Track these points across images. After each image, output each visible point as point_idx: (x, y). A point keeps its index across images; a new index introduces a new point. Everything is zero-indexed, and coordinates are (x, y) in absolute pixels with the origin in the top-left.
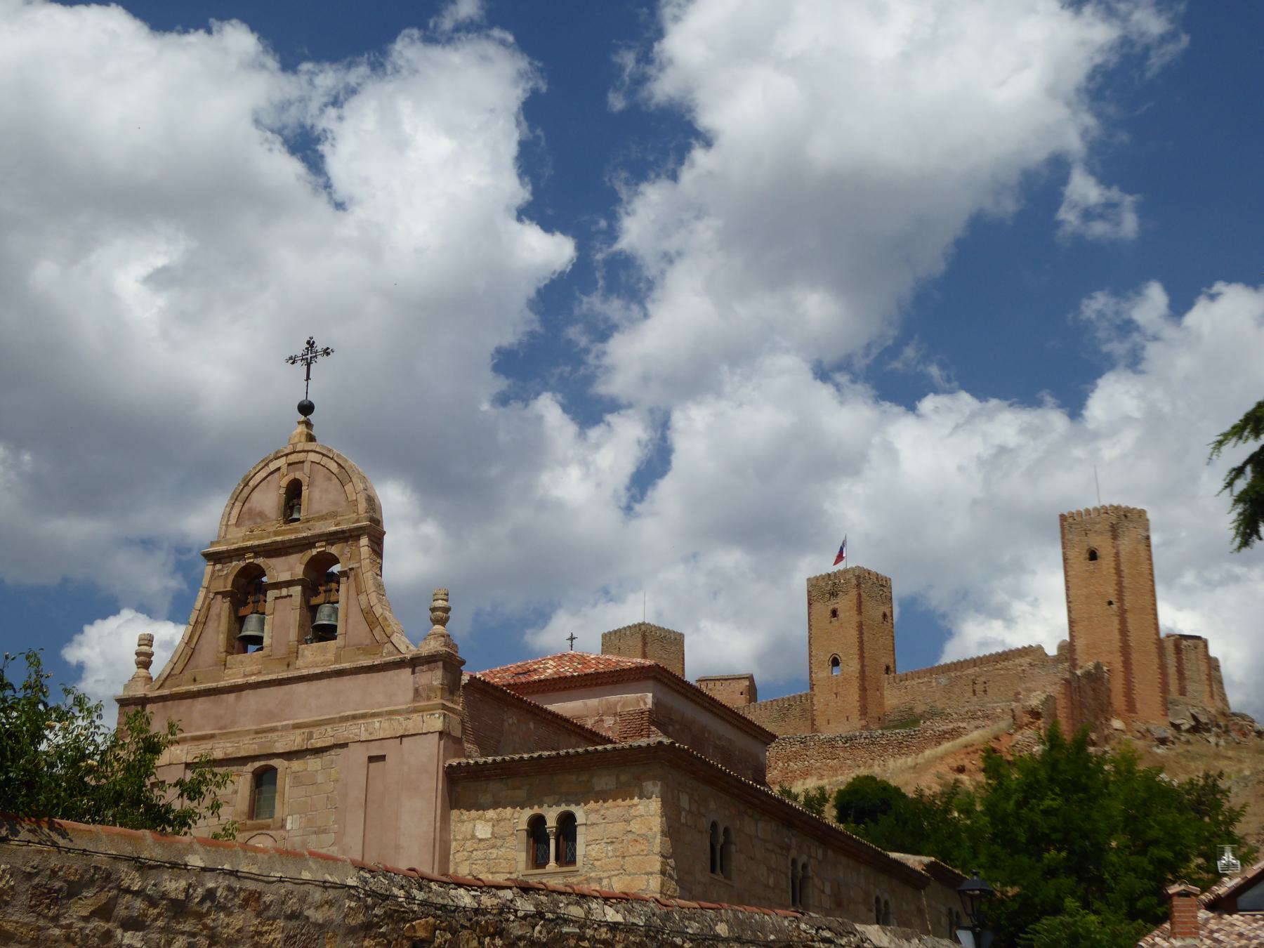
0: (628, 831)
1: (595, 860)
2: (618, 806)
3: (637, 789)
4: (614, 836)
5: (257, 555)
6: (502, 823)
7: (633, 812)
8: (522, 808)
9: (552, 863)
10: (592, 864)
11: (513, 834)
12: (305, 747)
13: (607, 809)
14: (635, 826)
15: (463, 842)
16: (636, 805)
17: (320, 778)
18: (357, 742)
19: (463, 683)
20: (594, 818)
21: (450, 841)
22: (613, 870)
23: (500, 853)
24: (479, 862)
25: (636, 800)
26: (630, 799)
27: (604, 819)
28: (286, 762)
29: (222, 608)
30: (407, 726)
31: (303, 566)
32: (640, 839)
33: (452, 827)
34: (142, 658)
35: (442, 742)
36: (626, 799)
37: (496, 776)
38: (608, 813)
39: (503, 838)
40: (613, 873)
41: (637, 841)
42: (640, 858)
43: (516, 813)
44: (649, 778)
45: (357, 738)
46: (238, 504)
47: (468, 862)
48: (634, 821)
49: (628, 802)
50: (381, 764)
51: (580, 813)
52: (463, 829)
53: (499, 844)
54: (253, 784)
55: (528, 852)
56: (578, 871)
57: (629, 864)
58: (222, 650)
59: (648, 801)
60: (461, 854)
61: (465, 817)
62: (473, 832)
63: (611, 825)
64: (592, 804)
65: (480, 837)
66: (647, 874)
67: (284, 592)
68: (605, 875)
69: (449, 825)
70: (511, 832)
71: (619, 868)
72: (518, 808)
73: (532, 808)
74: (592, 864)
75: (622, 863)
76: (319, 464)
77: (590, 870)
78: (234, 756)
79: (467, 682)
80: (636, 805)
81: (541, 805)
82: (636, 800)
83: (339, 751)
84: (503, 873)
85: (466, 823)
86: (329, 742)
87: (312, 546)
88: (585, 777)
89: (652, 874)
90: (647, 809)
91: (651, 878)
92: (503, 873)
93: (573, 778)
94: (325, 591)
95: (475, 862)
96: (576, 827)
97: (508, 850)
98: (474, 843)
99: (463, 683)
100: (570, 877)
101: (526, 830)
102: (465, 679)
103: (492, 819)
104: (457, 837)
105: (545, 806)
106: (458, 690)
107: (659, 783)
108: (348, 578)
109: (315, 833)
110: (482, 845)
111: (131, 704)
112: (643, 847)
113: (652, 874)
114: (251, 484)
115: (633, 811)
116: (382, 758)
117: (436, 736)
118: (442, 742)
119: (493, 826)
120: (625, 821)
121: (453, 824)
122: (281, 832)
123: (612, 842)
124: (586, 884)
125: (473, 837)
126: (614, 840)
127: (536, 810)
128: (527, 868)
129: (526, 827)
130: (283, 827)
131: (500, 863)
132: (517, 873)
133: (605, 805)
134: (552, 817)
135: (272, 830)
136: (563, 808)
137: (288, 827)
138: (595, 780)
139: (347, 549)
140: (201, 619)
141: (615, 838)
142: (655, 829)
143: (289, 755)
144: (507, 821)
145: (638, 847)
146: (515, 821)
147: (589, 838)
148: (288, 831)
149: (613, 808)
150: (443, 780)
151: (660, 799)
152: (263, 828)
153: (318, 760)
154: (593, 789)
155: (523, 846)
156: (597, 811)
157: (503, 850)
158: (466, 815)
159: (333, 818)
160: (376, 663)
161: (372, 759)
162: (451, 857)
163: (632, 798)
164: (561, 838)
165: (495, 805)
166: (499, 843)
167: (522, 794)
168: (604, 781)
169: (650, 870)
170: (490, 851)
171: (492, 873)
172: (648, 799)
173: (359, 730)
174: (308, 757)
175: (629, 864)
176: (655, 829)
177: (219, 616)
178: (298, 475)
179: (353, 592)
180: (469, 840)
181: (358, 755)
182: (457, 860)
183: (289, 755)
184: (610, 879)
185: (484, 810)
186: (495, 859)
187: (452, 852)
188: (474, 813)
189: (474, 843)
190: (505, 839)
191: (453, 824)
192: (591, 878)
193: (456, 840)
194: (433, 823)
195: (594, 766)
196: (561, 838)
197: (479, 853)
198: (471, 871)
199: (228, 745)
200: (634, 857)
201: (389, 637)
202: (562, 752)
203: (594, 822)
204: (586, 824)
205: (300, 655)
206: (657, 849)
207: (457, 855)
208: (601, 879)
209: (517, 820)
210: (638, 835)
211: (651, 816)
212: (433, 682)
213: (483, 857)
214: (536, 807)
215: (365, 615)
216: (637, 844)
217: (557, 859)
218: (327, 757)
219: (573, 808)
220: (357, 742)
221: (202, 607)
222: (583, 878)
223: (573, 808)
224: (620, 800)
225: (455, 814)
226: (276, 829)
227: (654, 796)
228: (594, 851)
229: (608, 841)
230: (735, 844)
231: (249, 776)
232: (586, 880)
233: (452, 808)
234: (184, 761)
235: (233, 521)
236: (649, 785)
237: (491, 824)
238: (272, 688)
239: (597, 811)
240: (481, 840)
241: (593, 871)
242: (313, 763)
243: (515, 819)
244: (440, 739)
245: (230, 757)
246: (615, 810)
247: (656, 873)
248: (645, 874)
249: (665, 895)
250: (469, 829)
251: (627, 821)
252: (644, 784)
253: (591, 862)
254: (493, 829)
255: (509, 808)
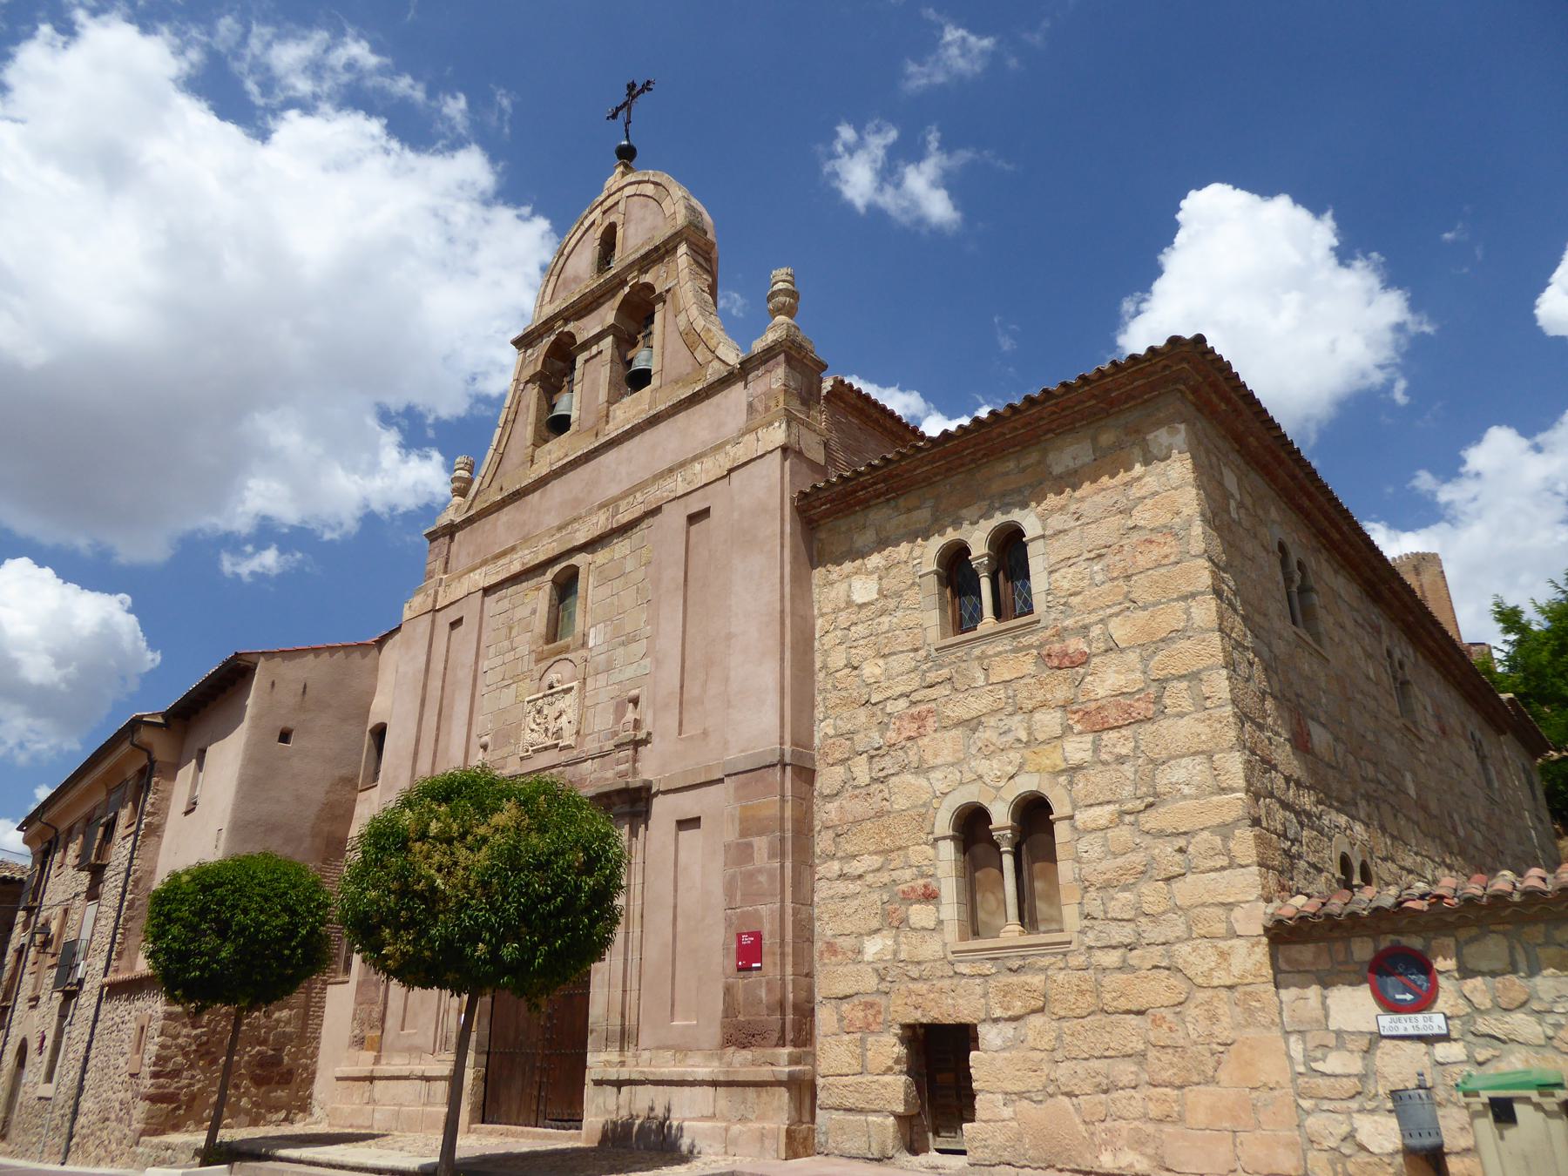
0: (1131, 529)
1: (1071, 595)
2: (1104, 490)
3: (1137, 451)
4: (1102, 543)
5: (567, 321)
6: (894, 571)
7: (1135, 492)
8: (926, 538)
9: (988, 622)
10: (1064, 604)
11: (913, 584)
12: (610, 527)
13: (1082, 499)
14: (1141, 516)
15: (834, 615)
16: (1139, 479)
17: (629, 565)
18: (674, 499)
19: (824, 392)
20: (1056, 522)
21: (813, 617)
22: (1109, 606)
23: (895, 620)
24: (861, 642)
25: (1138, 469)
26: (1126, 471)
27: (1078, 519)
28: (590, 556)
29: (533, 393)
30: (735, 453)
31: (614, 312)
32: (1159, 538)
33: (816, 596)
34: (457, 484)
35: (787, 463)
36: (1118, 473)
37: (878, 497)
38: (1085, 506)
39: (898, 594)
40: (1109, 611)
41: (1151, 542)
42: (1163, 570)
43: (916, 548)
44: (1159, 424)
45: (673, 495)
46: (553, 279)
47: (844, 646)
48: (1139, 508)
49: (1122, 477)
50: (704, 524)
51: (1029, 521)
52: (833, 595)
53: (892, 606)
54: (555, 597)
55: (942, 610)
56: (1038, 621)
57: (1141, 589)
58: (529, 443)
59: (1162, 465)
60: (830, 635)
61: (834, 576)
62: (848, 596)
63: (1094, 526)
64: (1052, 500)
65: (860, 601)
66: (1184, 598)
67: (594, 350)
68: (1094, 618)
69: (810, 590)
70: (911, 581)
71: (1121, 598)
72: (919, 539)
73: (942, 534)
74: (1064, 604)
75: (1126, 589)
76: (635, 195)
77: (1062, 616)
78: (532, 564)
79: (830, 388)
80: (1139, 479)
81: (957, 524)
82: (1138, 469)
83: (650, 521)
84: (902, 652)
85: (836, 585)
86: (637, 511)
87: (624, 283)
88: (1033, 457)
89: (1193, 595)
90: (1163, 479)
91: (1194, 603)
92: (902, 652)
93: (1012, 465)
94: (643, 337)
95: (855, 644)
96: (1025, 545)
97: (909, 612)
98: (851, 613)
99: (824, 392)
100: (1024, 635)
101: (936, 572)
102: (827, 385)
103: (878, 568)
104: (824, 611)
105: (966, 525)
106: (819, 403)
107: (1182, 427)
108: (665, 302)
109: (623, 644)
110: (864, 614)
111: (439, 537)
112: (1166, 550)
113: (1193, 595)
114: (566, 252)
115: (1134, 490)
116: (705, 513)
117: (778, 454)
118: (787, 463)
119: (880, 578)
120: (1121, 512)
121: (817, 590)
122: (583, 652)
123: (1100, 556)
124: (1058, 642)
125: (849, 603)
126: (1103, 551)
127: (951, 535)
128: (944, 635)
129: (935, 568)
130: (584, 645)
131: (897, 637)
132: (927, 648)
133: (1077, 494)
134: (978, 541)
135: (572, 651)
136: (999, 519)
137: (591, 644)
138: (1051, 456)
139: (664, 269)
140: (511, 417)
141: (1106, 547)
142: (1186, 511)
143: (590, 546)
144: (902, 566)
145: (1156, 552)
146: (916, 562)
147: (1053, 559)
148: (591, 649)
149: (1094, 497)
150: (792, 520)
151: (1188, 455)
152: (560, 653)
153: (627, 541)
154: (1051, 473)
155: (934, 600)
156: (1062, 508)
157: (899, 614)
158: (835, 571)
159: (644, 617)
160: (697, 389)
161: (693, 519)
162: (817, 644)
163: (1129, 468)
164: (1001, 575)
165: (882, 544)
166: (892, 603)
167: (923, 515)
168: (1069, 454)
169: (1190, 589)
170: (878, 620)
171: (884, 656)
172: (1162, 460)
173: (678, 484)
174: (615, 541)
175: (1141, 589)
176: (1186, 511)
177: (528, 407)
178: (613, 218)
179: (670, 316)
180: (842, 610)
181: (675, 517)
182: (825, 648)
183: (590, 546)
184: (1106, 625)
185: (863, 558)
186: (887, 632)
187: (817, 636)
188: (848, 566)
189: (851, 613)
190: (901, 596)
191: (816, 590)
192: (1065, 629)
193: (822, 615)
194: (778, 586)
195: (1049, 431)
196: (1001, 575)
197: (860, 627)
198: (848, 659)
199: (527, 552)
200: (1150, 572)
201: (713, 352)
202: (983, 413)
203: (1060, 527)
204: (1043, 537)
205: (611, 419)
206: (1198, 545)
207: (825, 639)
208: (1086, 627)
209: (919, 560)
210: (1151, 530)
211: (1173, 488)
212: (773, 387)
213: (867, 632)
214: (949, 530)
215: (685, 337)
216: (1152, 547)
217: (998, 614)
218: (637, 535)
219: (1016, 515)
220: (674, 499)
221: (512, 403)
222: (1049, 632)
223: (1016, 515)
224: (1105, 479)
225: (818, 574)
226: (576, 650)
227: (1175, 451)
228: (1065, 580)
229: (1092, 555)
230: (1317, 593)
231: (548, 587)
232: (1057, 634)
233: (813, 567)
234: (481, 586)
235: (547, 299)
236: (1160, 437)
237: (876, 576)
238: (578, 469)
239: (1062, 508)
240: (861, 606)
241: (1070, 616)
242: (621, 547)
243: (915, 559)
244: (784, 458)
245: (528, 566)
246: (1098, 498)
247: (1202, 593)
248: (1177, 600)
249: (1229, 636)
250: (841, 594)
251: (1126, 512)
252: (1150, 437)
253: (1062, 601)
254: (880, 584)
255: (904, 544)
